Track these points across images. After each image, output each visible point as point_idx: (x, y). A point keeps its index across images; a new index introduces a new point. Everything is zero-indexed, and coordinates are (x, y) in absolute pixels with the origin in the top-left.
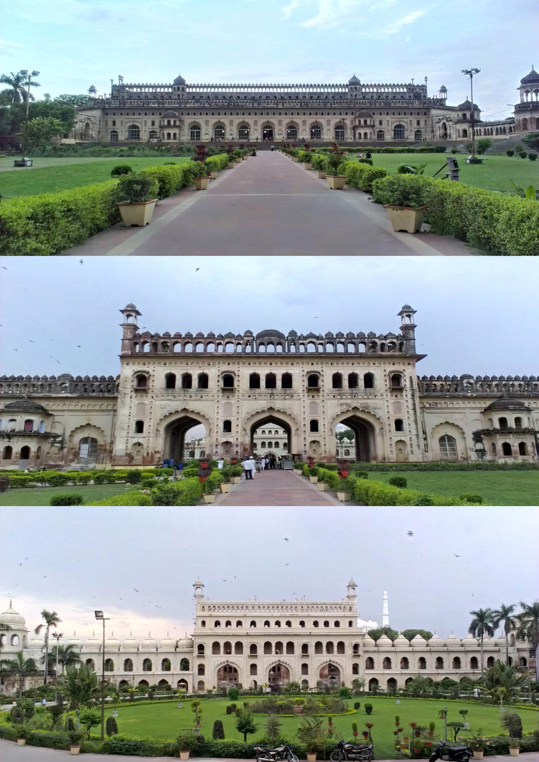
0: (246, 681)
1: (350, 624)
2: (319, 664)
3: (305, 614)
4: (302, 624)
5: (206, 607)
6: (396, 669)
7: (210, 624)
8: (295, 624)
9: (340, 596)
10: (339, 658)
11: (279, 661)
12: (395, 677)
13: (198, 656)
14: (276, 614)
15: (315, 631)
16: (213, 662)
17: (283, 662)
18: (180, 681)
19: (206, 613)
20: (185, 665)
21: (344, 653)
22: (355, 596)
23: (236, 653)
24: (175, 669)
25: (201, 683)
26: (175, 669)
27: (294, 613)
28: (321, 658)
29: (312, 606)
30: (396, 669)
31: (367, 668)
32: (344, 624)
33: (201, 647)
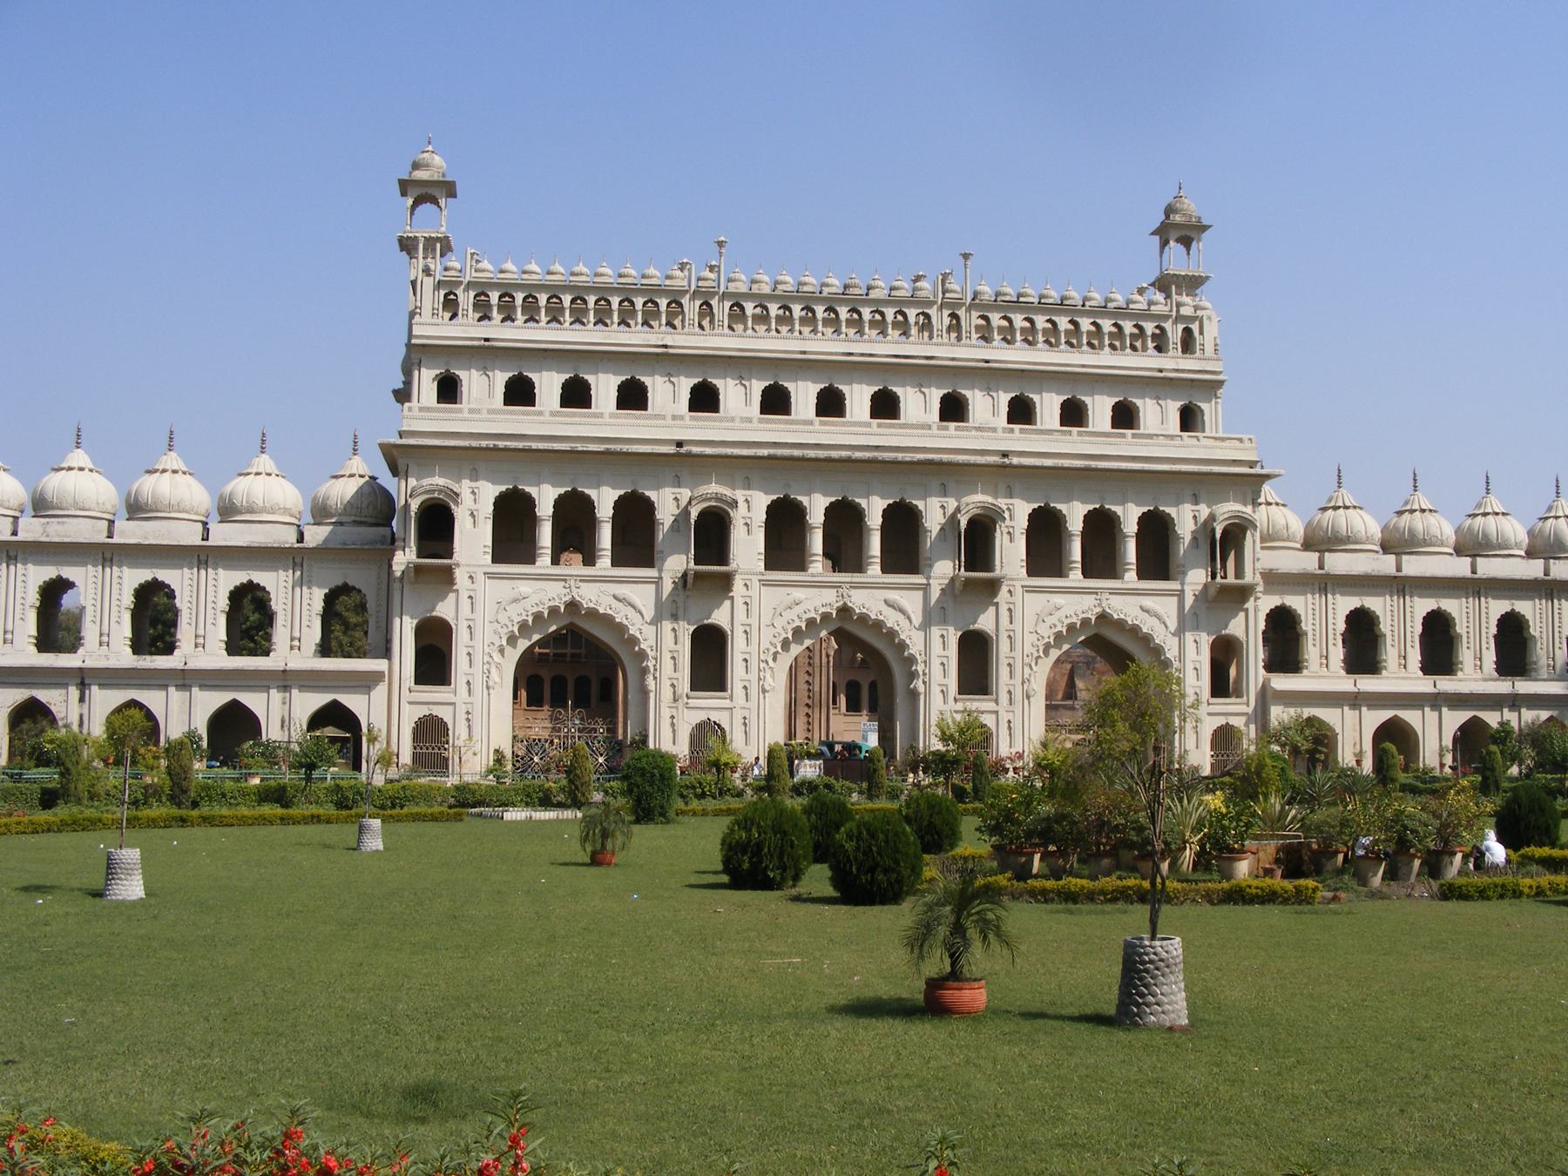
0: (670, 720)
1: (1189, 419)
2: (1048, 634)
3: (970, 352)
4: (953, 409)
5: (466, 299)
6: (1402, 670)
7: (483, 388)
8: (920, 405)
9: (1122, 271)
10: (1148, 602)
11: (845, 611)
12: (1411, 717)
13: (418, 569)
14: (825, 345)
15: (1021, 442)
16: (496, 609)
17: (863, 618)
18: (318, 719)
19: (467, 329)
20: (347, 624)
21: (1166, 577)
22: (1193, 284)
23: (621, 557)
24: (295, 644)
25: (431, 732)
26: (295, 644)
27: (915, 348)
28: (1059, 599)
29: (1002, 314)
30: (1402, 670)
31: (1273, 666)
32: (1158, 415)
33: (437, 524)
